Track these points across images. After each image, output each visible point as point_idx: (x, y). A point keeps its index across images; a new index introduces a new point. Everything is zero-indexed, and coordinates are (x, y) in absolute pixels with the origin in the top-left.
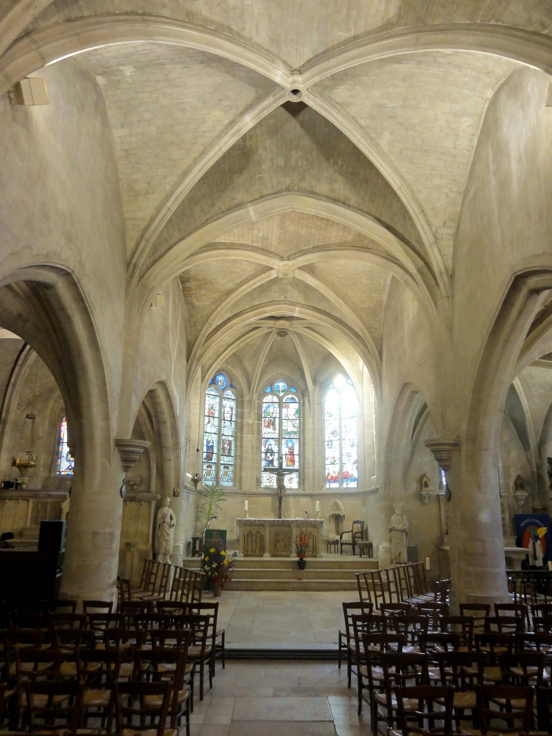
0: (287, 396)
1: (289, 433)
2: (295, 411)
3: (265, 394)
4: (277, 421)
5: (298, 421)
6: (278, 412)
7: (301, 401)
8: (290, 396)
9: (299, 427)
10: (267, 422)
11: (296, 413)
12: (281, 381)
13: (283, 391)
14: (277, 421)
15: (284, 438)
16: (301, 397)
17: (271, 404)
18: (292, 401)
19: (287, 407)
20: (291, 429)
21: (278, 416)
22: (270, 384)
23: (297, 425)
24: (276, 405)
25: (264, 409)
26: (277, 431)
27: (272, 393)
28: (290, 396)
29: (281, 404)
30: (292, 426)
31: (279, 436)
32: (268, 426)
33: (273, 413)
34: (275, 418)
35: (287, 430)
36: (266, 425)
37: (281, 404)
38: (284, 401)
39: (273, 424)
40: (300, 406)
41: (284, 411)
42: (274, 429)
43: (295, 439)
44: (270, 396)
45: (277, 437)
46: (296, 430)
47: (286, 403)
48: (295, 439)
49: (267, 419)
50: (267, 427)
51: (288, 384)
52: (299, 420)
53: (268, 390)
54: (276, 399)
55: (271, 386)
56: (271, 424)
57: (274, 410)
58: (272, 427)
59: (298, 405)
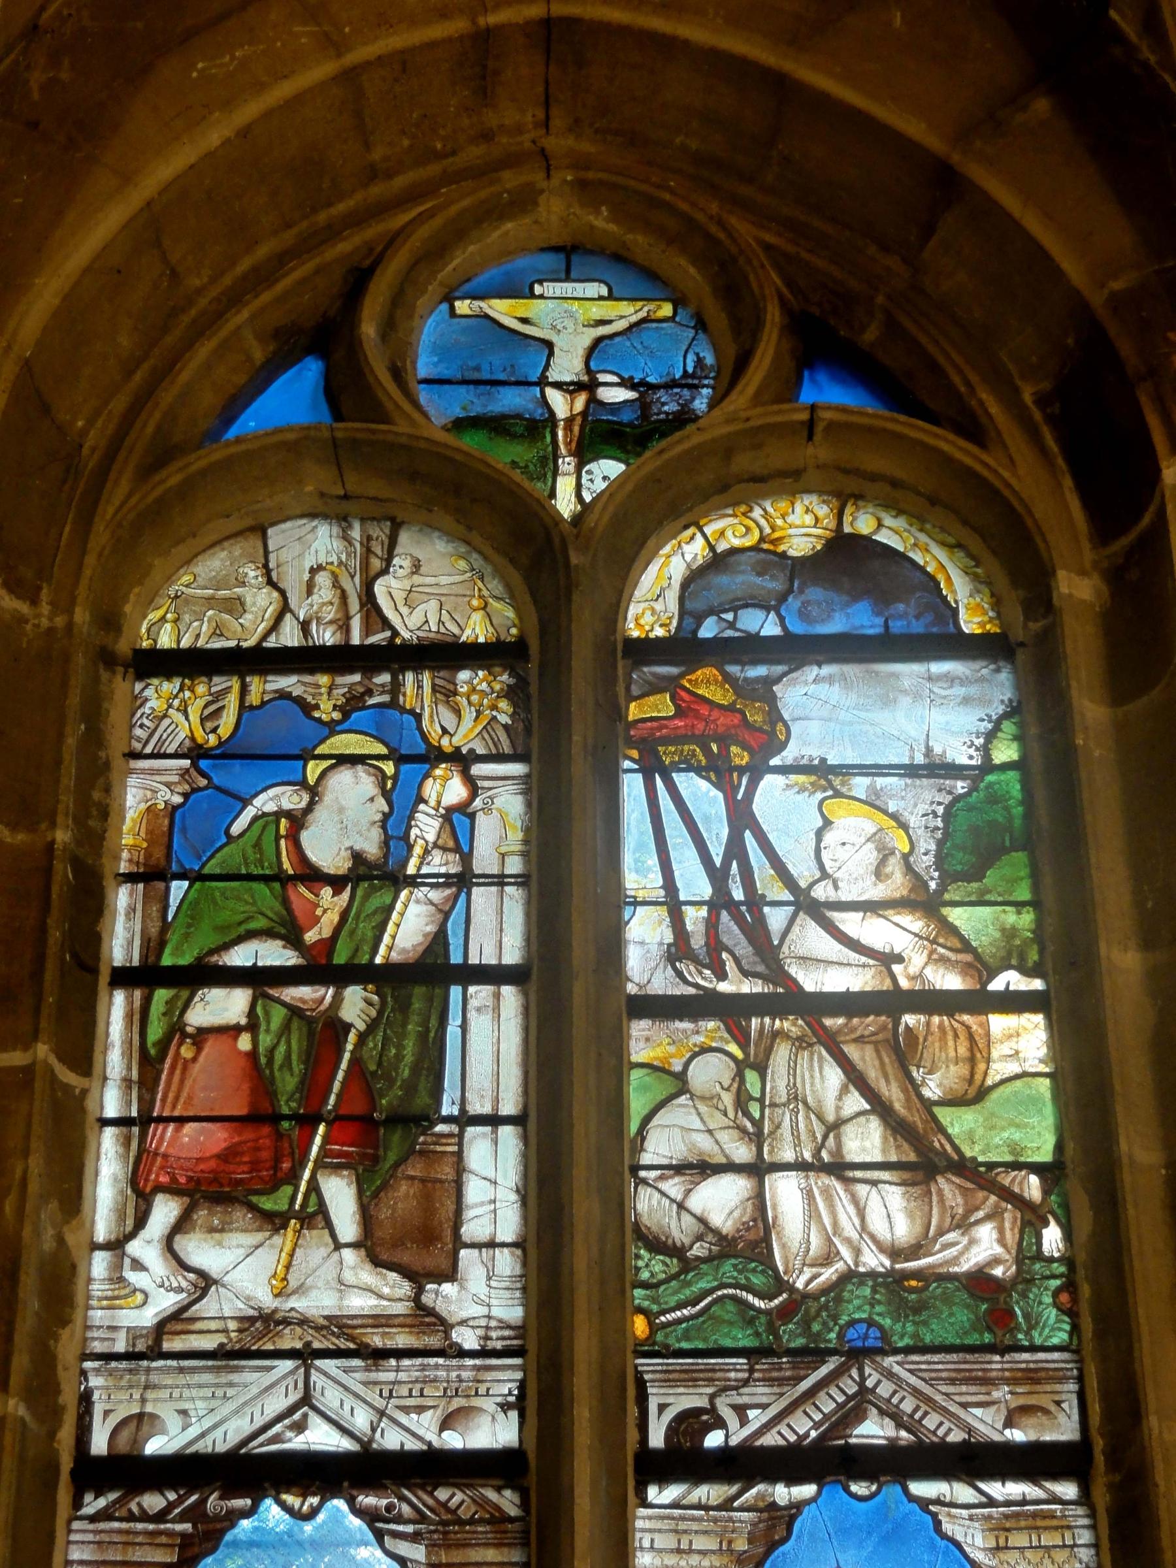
0: (730, 530)
1: (798, 1333)
2: (920, 804)
3: (198, 489)
4: (488, 1046)
5: (1022, 1043)
6: (502, 825)
7: (1077, 588)
8: (802, 525)
9: (1086, 1169)
10: (209, 1081)
11: (969, 852)
12: (572, 256)
13: (599, 434)
14: (488, 1046)
15: (684, 1460)
16: (1055, 507)
17: (325, 692)
18: (861, 618)
19: (739, 746)
20: (845, 1224)
21: (498, 929)
22: (302, 286)
23: (1023, 1127)
24: (467, 712)
25: (141, 795)
26: (482, 1295)
27: (393, 471)
28: (802, 525)
29: (571, 694)
30: (866, 1141)
31: (543, 1402)
32: (244, 1182)
33: (378, 875)
34: (436, 972)
35: (752, 1243)
36: (193, 1142)
37: (571, 694)
38: (651, 604)
39: (392, 1128)
40: (1041, 708)
41: (660, 845)
42: (418, 1243)
43: (975, 1461)
44: (313, 546)
45: (494, 1432)
46: (985, 1247)
47: (683, 648)
48: (975, 1461)
49: (224, 1006)
50: (213, 1193)
51: (726, 305)
52: (1072, 1008)
53: (292, 399)
54: (435, 588)
55: (325, 335)
56: (336, 1112)
57: (421, 831)
58: (340, 1196)
59: (999, 686)
